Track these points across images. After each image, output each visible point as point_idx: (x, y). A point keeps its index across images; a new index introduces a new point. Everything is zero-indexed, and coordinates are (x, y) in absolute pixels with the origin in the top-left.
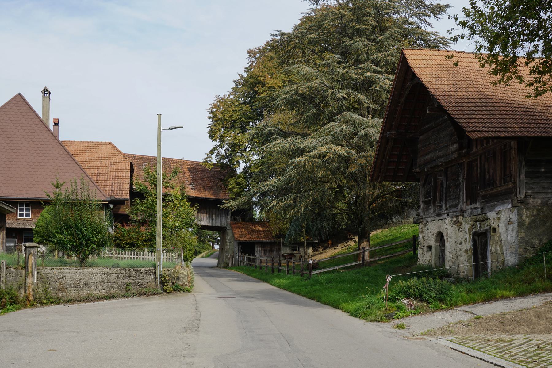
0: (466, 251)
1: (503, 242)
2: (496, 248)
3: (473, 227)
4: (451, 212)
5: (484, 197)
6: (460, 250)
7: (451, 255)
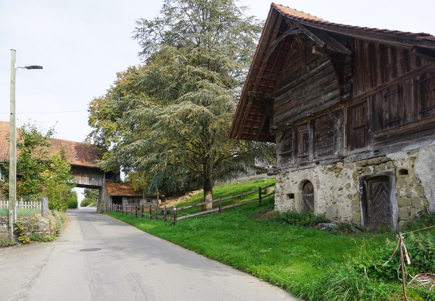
0: (350, 196)
1: (423, 185)
3: (360, 172)
4: (322, 160)
5: (379, 139)
7: (324, 201)
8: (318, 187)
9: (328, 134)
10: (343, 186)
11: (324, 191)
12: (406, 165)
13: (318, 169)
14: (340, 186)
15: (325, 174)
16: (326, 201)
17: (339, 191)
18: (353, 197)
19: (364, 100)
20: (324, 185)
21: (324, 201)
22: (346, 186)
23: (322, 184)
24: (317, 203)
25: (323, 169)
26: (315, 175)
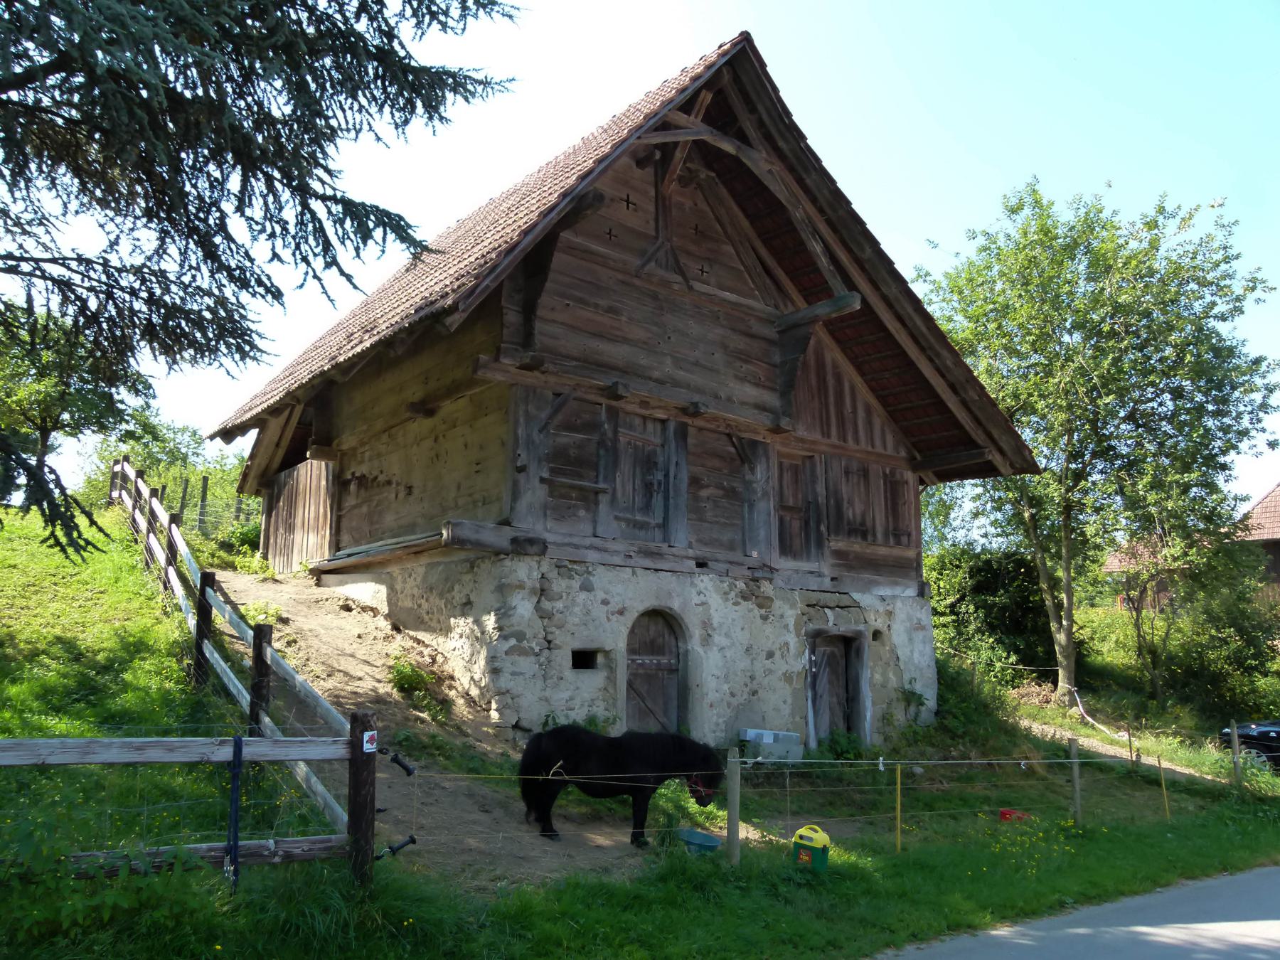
0: (788, 677)
1: (901, 665)
2: (884, 674)
4: (716, 560)
5: (838, 554)
6: (769, 672)
7: (726, 687)
8: (707, 640)
9: (723, 488)
10: (773, 648)
11: (728, 655)
12: (879, 624)
13: (706, 581)
14: (768, 645)
15: (734, 604)
17: (767, 659)
18: (795, 678)
19: (811, 454)
20: (727, 635)
21: (726, 687)
22: (780, 649)
23: (723, 632)
24: (705, 690)
25: (727, 589)
26: (696, 599)
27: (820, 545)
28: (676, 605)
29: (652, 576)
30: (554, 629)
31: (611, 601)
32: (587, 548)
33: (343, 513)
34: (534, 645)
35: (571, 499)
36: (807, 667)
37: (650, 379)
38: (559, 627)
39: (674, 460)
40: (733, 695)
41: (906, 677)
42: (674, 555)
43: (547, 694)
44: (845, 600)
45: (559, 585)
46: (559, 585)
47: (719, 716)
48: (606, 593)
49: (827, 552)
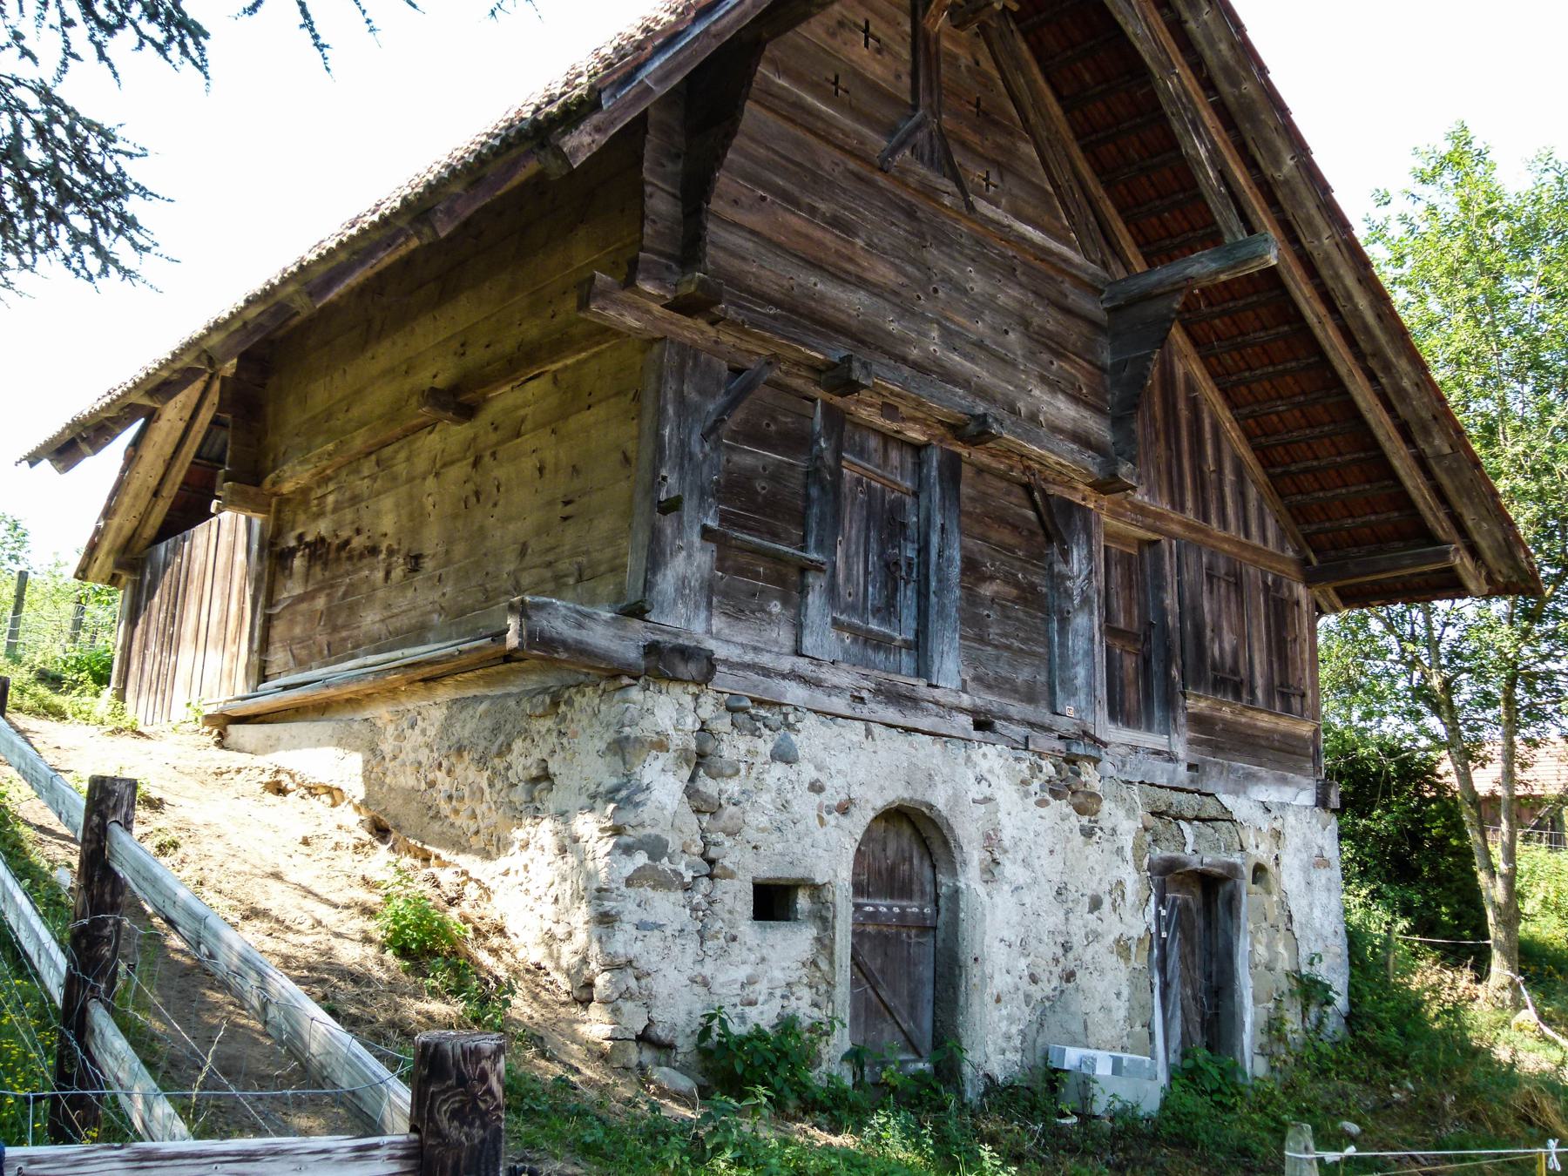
0: (1122, 948)
1: (1296, 928)
2: (1270, 946)
4: (1009, 719)
5: (1199, 722)
6: (1093, 936)
8: (991, 869)
11: (1027, 900)
12: (1261, 852)
13: (991, 757)
14: (1093, 887)
16: (1029, 960)
17: (1091, 911)
18: (1134, 949)
19: (1155, 537)
22: (1110, 893)
23: (1020, 856)
25: (1027, 774)
26: (976, 791)
27: (1169, 704)
28: (939, 799)
29: (900, 740)
30: (721, 837)
31: (828, 785)
32: (784, 677)
33: (276, 610)
34: (682, 868)
35: (756, 576)
36: (1153, 929)
37: (904, 360)
38: (731, 834)
39: (938, 520)
40: (1034, 979)
41: (1304, 952)
42: (937, 703)
43: (708, 969)
44: (1211, 809)
45: (734, 746)
46: (734, 746)
47: (1011, 1019)
48: (819, 768)
49: (1182, 719)
